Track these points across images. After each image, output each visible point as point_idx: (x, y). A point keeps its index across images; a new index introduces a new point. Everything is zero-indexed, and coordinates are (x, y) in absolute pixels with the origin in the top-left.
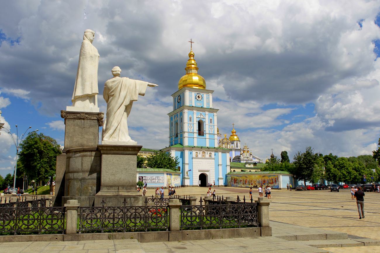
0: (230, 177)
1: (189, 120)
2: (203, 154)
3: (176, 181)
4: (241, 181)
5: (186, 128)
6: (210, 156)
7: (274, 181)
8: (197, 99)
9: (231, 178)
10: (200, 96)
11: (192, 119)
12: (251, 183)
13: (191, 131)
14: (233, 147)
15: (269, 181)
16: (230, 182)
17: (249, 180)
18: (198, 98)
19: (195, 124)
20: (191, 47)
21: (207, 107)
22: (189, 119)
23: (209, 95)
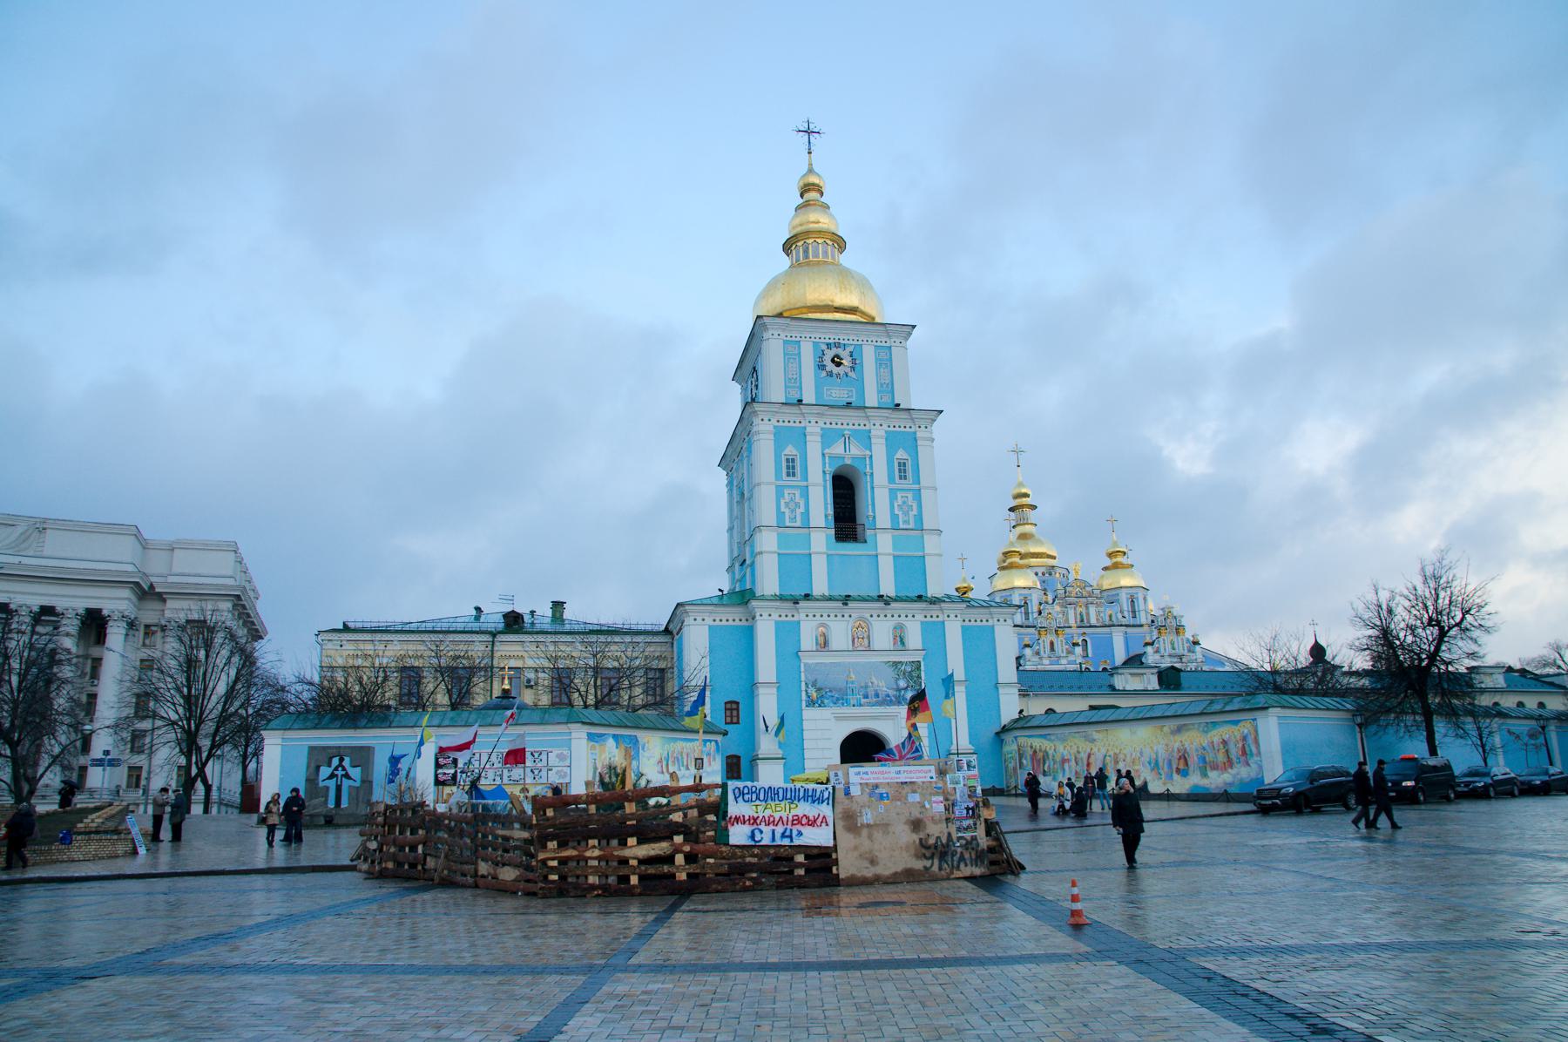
0: (1015, 747)
1: (784, 470)
2: (860, 632)
4: (1064, 761)
5: (766, 507)
7: (1234, 752)
9: (1019, 749)
10: (844, 354)
11: (798, 464)
13: (798, 524)
14: (1114, 619)
16: (1015, 769)
18: (830, 366)
19: (815, 485)
20: (810, 153)
22: (784, 464)
23: (890, 347)
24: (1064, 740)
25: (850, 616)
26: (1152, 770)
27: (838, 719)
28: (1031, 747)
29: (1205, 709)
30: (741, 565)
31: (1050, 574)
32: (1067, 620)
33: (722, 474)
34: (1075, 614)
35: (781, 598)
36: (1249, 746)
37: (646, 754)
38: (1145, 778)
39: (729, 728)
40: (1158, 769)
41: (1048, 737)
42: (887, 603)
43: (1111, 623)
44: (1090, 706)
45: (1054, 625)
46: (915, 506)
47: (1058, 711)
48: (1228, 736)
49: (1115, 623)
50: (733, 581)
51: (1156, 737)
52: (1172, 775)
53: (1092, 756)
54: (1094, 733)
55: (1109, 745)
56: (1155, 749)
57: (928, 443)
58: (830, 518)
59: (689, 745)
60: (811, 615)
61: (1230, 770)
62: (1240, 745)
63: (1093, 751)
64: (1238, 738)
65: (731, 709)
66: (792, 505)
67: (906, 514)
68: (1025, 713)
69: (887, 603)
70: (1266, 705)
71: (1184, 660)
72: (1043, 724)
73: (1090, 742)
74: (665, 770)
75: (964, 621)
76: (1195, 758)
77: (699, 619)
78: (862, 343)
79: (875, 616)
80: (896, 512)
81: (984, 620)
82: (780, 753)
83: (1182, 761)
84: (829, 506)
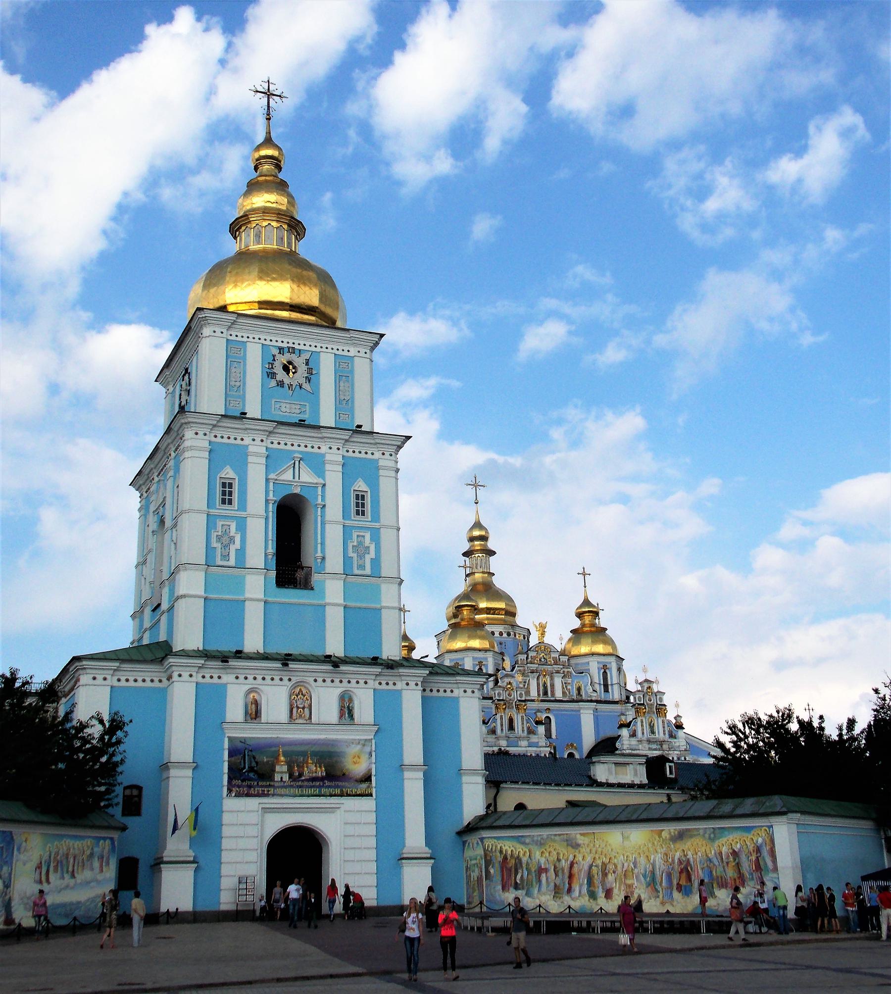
0: (480, 851)
3: (72, 882)
4: (541, 870)
6: (347, 710)
7: (747, 866)
8: (279, 378)
9: (486, 855)
10: (299, 361)
12: (603, 883)
14: (583, 693)
15: (718, 872)
17: (591, 867)
18: (281, 375)
19: (253, 516)
21: (338, 416)
22: (218, 489)
24: (541, 844)
25: (290, 680)
26: (648, 885)
27: (266, 810)
28: (501, 852)
29: (711, 811)
30: (154, 610)
31: (509, 634)
32: (528, 693)
33: (134, 498)
34: (538, 685)
35: (206, 654)
37: (22, 857)
38: (639, 896)
39: (130, 821)
41: (523, 839)
42: (336, 665)
43: (580, 698)
44: (567, 801)
45: (515, 696)
46: (372, 548)
47: (530, 807)
48: (738, 846)
49: (584, 697)
50: (142, 631)
51: (654, 843)
52: (671, 893)
53: (575, 865)
54: (578, 836)
57: (393, 474)
58: (270, 557)
59: (78, 842)
60: (242, 677)
63: (576, 859)
64: (751, 849)
65: (132, 796)
66: (225, 540)
67: (361, 557)
69: (336, 665)
70: (784, 809)
71: (665, 747)
72: (516, 823)
73: (573, 847)
74: (44, 878)
75: (424, 690)
76: (700, 871)
77: (100, 678)
78: (322, 350)
79: (320, 680)
80: (351, 554)
81: (448, 690)
82: (190, 855)
83: (684, 875)
84: (270, 542)
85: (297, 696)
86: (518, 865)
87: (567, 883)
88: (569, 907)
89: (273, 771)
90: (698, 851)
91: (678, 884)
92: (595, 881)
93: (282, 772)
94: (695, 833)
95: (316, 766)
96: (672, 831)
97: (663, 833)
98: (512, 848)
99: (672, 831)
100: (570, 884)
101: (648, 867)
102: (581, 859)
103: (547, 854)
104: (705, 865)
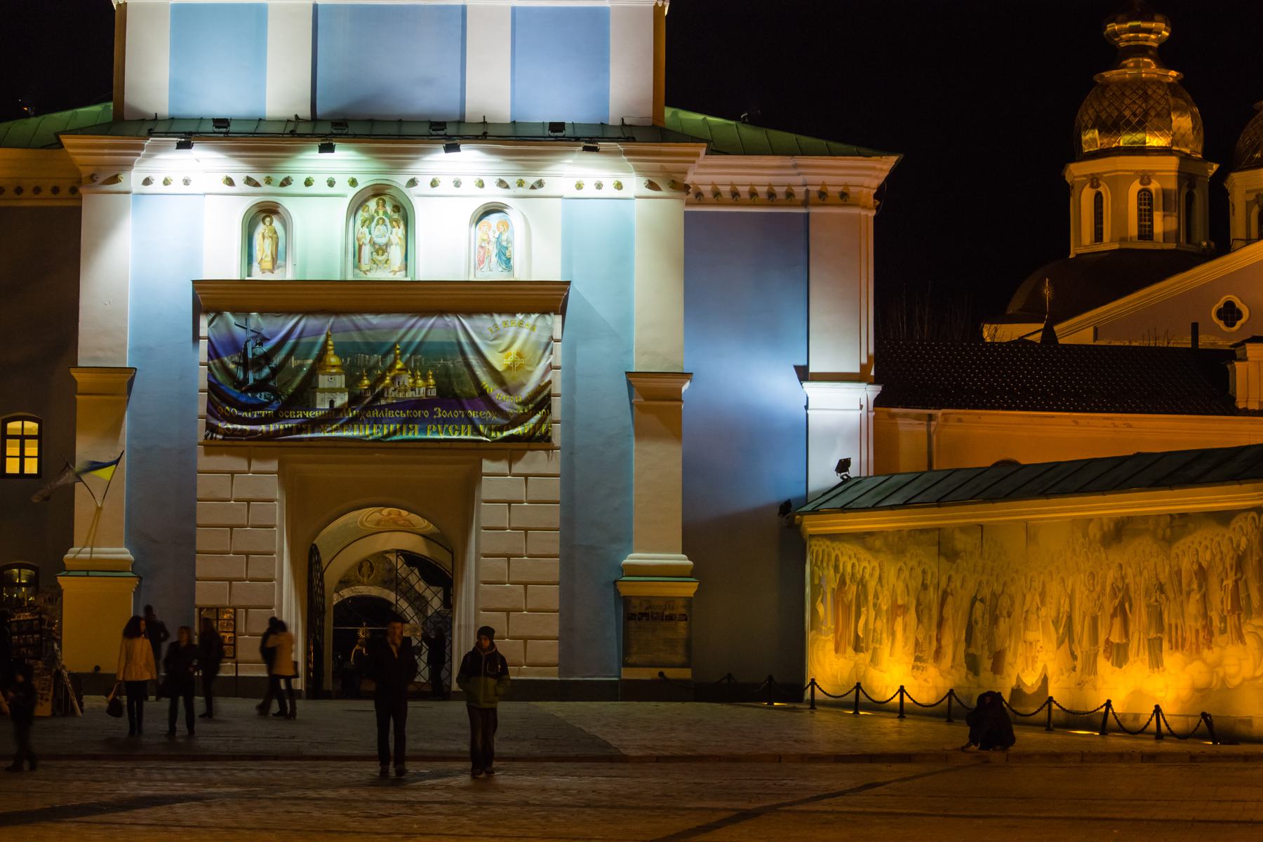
26: (1060, 643)
28: (836, 568)
36: (1247, 589)
38: (1045, 667)
40: (1071, 641)
41: (870, 540)
48: (1208, 556)
51: (1074, 550)
52: (1095, 661)
53: (950, 599)
55: (984, 568)
56: (1069, 582)
61: (1206, 653)
62: (1229, 583)
63: (952, 585)
64: (1228, 561)
68: (853, 471)
83: (1118, 622)
85: (373, 218)
86: (862, 597)
87: (935, 638)
88: (902, 690)
89: (314, 387)
90: (1145, 568)
91: (1107, 641)
92: (979, 634)
93: (333, 390)
94: (1143, 527)
95: (413, 376)
96: (1105, 521)
97: (1091, 525)
98: (854, 560)
99: (1105, 521)
100: (939, 640)
101: (1062, 601)
102: (959, 585)
103: (906, 573)
104: (1153, 599)
